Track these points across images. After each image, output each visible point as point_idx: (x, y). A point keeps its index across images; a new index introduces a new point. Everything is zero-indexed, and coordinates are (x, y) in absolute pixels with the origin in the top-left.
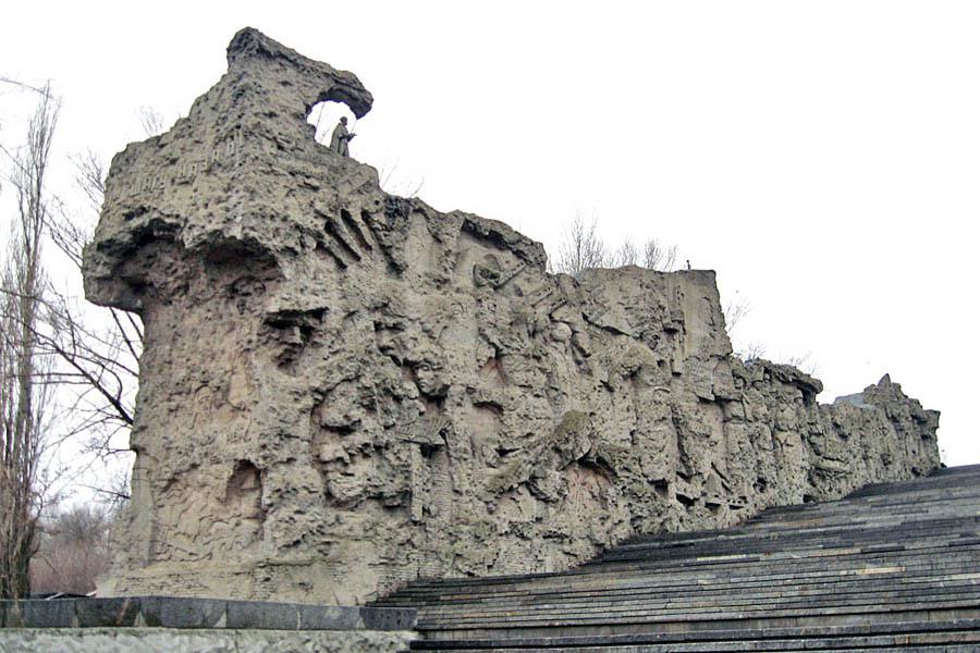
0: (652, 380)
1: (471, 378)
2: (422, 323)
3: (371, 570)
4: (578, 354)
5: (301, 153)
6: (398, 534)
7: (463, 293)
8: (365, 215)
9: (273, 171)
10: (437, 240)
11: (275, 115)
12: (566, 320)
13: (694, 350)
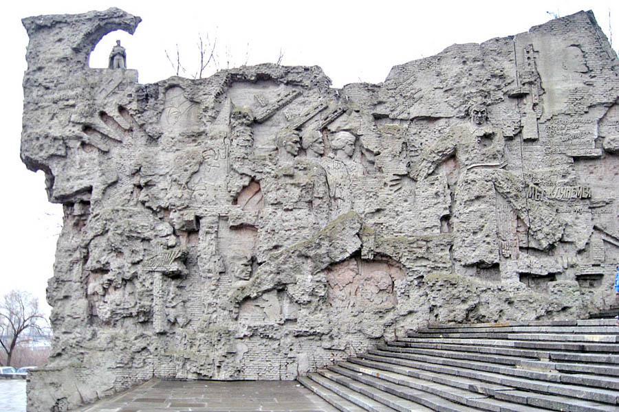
0: (467, 159)
1: (224, 207)
2: (170, 176)
3: (110, 372)
4: (367, 154)
6: (134, 344)
8: (122, 109)
10: (193, 102)
11: (44, 68)
12: (345, 128)
13: (561, 106)
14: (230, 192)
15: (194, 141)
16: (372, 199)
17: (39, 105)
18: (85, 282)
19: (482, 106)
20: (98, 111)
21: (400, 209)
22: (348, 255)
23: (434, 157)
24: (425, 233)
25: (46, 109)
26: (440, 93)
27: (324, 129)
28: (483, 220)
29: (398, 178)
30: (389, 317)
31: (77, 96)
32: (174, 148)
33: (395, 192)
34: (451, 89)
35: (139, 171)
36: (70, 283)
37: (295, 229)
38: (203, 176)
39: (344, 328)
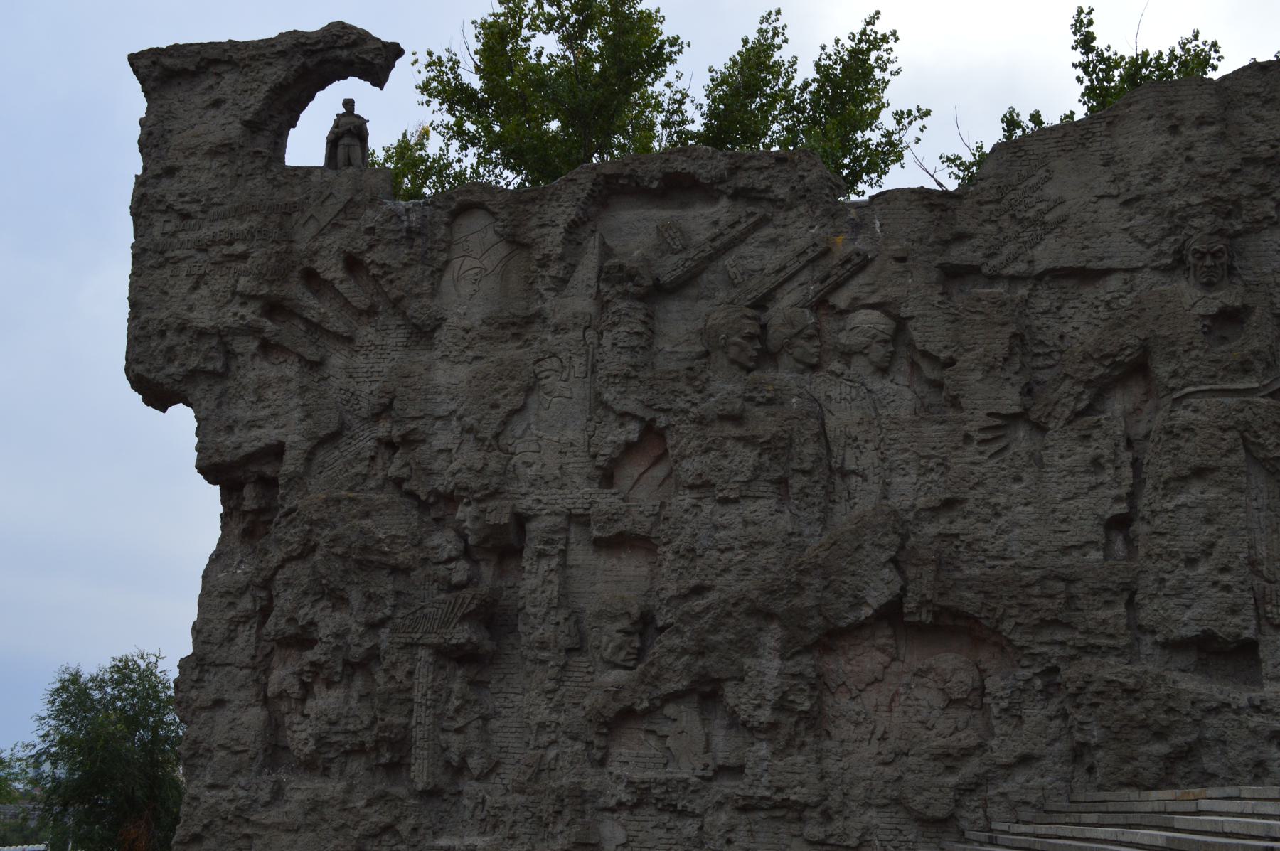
0: (1175, 374)
1: (579, 494)
2: (460, 418)
4: (925, 366)
5: (220, 209)
6: (365, 817)
7: (566, 331)
8: (353, 264)
9: (167, 259)
11: (178, 169)
12: (875, 299)
14: (594, 456)
15: (516, 336)
16: (934, 476)
17: (167, 255)
18: (261, 666)
19: (1216, 238)
20: (299, 268)
21: (1002, 500)
22: (866, 612)
23: (1092, 370)
24: (1066, 561)
25: (184, 265)
26: (1109, 208)
27: (820, 304)
28: (1211, 529)
29: (998, 422)
30: (971, 768)
31: (249, 236)
32: (470, 353)
33: (992, 456)
34: (1138, 198)
35: (388, 407)
36: (228, 669)
37: (742, 548)
38: (533, 419)
39: (858, 791)
